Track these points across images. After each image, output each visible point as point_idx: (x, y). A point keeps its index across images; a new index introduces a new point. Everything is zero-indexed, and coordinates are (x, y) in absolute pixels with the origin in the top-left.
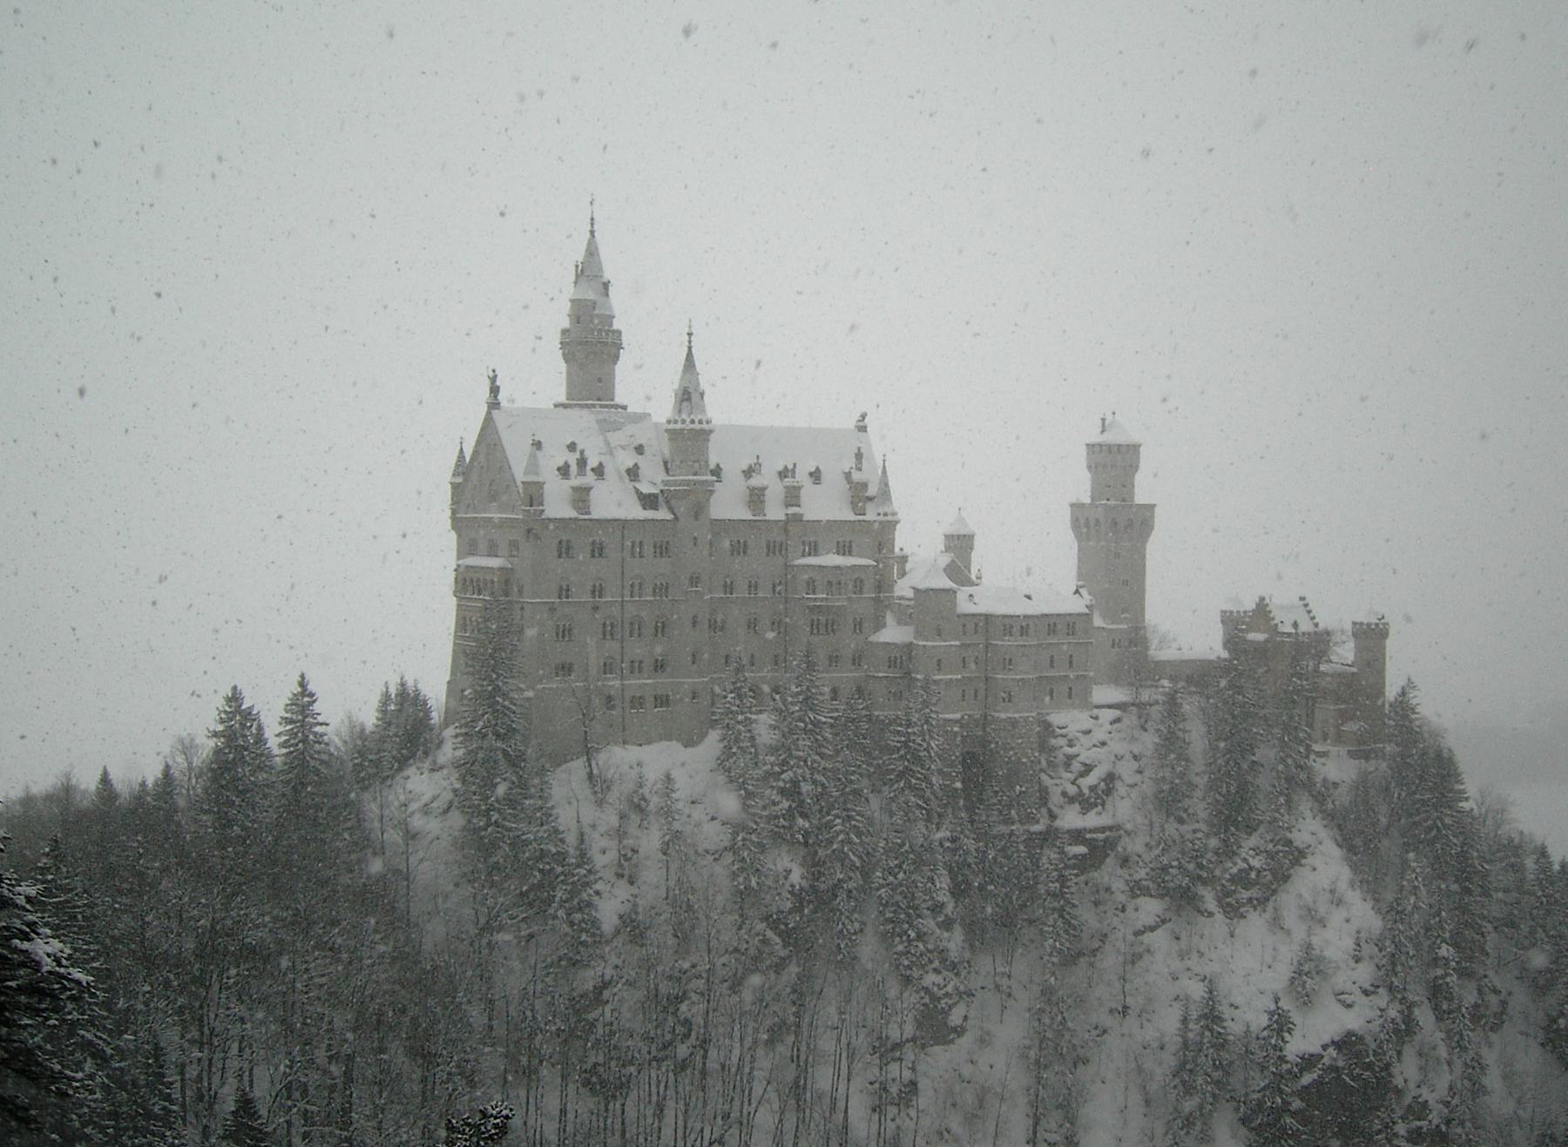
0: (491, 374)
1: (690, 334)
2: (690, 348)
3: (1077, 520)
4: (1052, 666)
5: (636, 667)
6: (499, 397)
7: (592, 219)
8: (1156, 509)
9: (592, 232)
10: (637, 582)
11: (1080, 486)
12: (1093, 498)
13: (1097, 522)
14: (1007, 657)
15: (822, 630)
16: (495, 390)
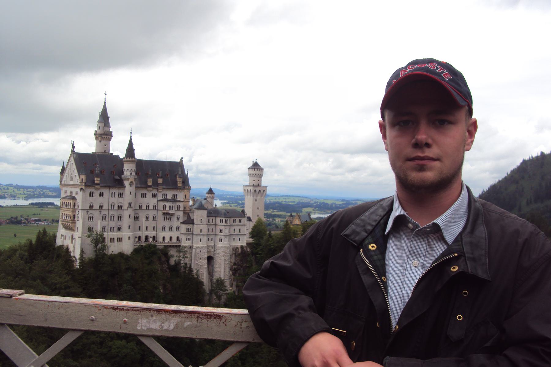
0: (72, 143)
1: (131, 133)
2: (131, 137)
3: (245, 190)
4: (234, 232)
5: (112, 229)
6: (75, 150)
7: (105, 99)
8: (268, 187)
9: (105, 103)
10: (113, 204)
11: (246, 180)
12: (249, 184)
13: (251, 190)
14: (221, 229)
15: (167, 220)
16: (73, 147)
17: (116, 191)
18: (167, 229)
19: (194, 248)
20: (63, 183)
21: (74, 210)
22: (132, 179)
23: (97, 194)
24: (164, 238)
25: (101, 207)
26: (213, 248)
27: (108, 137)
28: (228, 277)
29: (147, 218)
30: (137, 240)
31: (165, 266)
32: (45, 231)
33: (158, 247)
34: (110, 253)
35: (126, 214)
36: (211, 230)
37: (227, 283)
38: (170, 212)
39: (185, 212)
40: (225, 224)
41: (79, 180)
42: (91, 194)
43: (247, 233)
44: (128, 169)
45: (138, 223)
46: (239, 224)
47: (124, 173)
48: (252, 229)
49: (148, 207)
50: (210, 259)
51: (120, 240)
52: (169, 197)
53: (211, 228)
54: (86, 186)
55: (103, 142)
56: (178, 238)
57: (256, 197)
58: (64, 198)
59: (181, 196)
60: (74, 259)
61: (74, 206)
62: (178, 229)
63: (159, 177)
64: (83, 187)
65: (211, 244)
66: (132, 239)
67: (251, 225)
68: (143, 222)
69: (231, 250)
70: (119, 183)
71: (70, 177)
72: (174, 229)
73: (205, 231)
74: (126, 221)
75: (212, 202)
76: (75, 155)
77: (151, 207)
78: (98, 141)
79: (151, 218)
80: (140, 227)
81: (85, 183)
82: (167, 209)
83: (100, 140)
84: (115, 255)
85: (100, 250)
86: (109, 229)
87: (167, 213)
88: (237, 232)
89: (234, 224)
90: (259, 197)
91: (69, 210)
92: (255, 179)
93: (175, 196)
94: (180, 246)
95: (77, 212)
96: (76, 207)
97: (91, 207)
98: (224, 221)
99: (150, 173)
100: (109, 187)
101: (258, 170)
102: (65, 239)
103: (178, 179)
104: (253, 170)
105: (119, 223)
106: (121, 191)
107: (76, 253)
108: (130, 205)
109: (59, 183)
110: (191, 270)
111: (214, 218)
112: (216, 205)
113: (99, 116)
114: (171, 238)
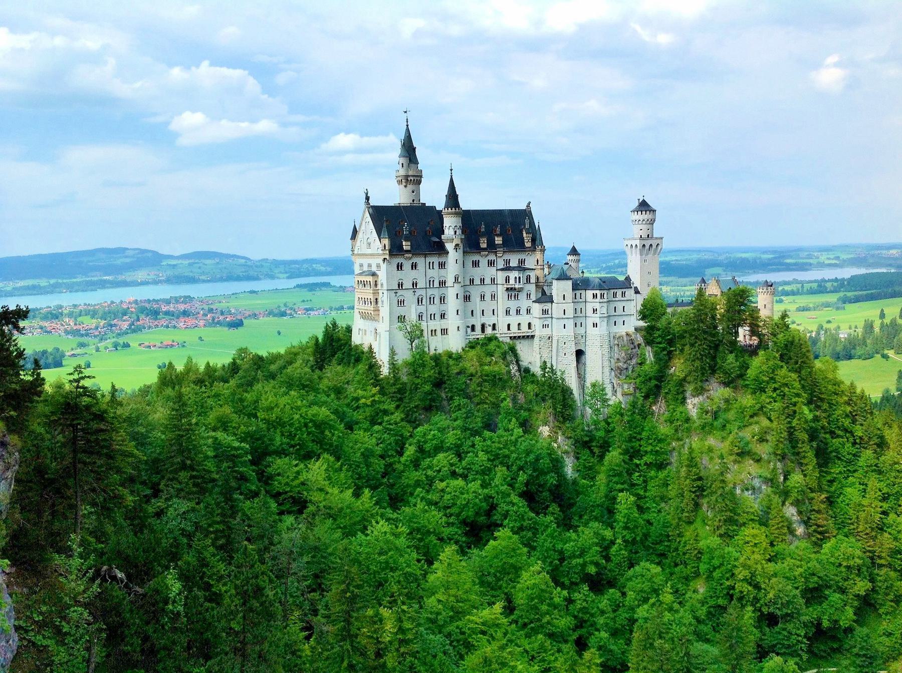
5: (432, 317)
9: (407, 125)
16: (367, 198)
17: (435, 260)
18: (513, 312)
19: (555, 339)
20: (356, 252)
21: (376, 293)
22: (457, 241)
23: (407, 265)
24: (509, 325)
25: (415, 285)
26: (584, 337)
27: (416, 179)
28: (607, 381)
29: (483, 297)
30: (469, 330)
31: (514, 368)
32: (335, 325)
33: (501, 339)
34: (432, 352)
35: (452, 292)
36: (579, 310)
37: (609, 390)
38: (517, 286)
39: (537, 285)
40: (601, 301)
41: (381, 246)
42: (400, 267)
43: (633, 311)
44: (451, 225)
45: (470, 306)
46: (623, 299)
47: (446, 231)
48: (642, 305)
50: (579, 354)
51: (444, 332)
52: (514, 263)
53: (578, 307)
54: (391, 254)
55: (410, 187)
56: (529, 324)
57: (647, 254)
58: (361, 274)
59: (530, 262)
60: (381, 363)
61: (376, 285)
62: (528, 311)
63: (498, 235)
64: (387, 257)
65: (581, 331)
66: (462, 329)
67: (639, 300)
68: (477, 304)
69: (612, 338)
70: (439, 249)
71: (365, 243)
72: (523, 311)
73: (570, 313)
74: (453, 304)
75: (578, 267)
76: (371, 210)
77: (488, 281)
78: (402, 186)
80: (472, 311)
81: (390, 251)
82: (512, 281)
83: (404, 184)
84: (440, 354)
85: (417, 348)
86: (429, 316)
87: (512, 288)
88: (620, 311)
89: (614, 299)
90: (650, 256)
91: (368, 291)
92: (641, 227)
93: (522, 262)
94: (533, 337)
95: (381, 294)
96: (379, 287)
97: (400, 285)
98: (599, 296)
99: (483, 230)
100: (425, 256)
101: (648, 212)
102: (365, 334)
103: (525, 235)
104: (640, 213)
105: (443, 307)
106: (442, 260)
107: (383, 357)
108: (456, 279)
109: (351, 253)
110: (552, 370)
111: (583, 292)
112: (583, 272)
113: (400, 147)
114: (519, 324)
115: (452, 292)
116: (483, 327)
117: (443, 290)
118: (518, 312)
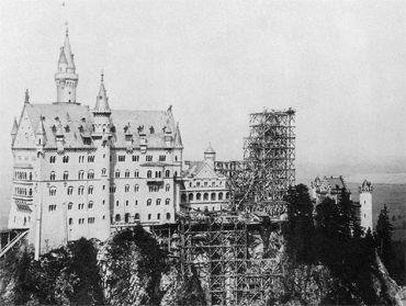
5: (81, 206)
16: (27, 98)
18: (154, 202)
23: (59, 159)
24: (150, 216)
25: (66, 176)
29: (127, 189)
38: (158, 180)
42: (53, 160)
49: (127, 174)
61: (31, 177)
68: (120, 195)
74: (101, 194)
79: (132, 189)
82: (153, 175)
97: (53, 177)
115: (100, 183)
116: (127, 215)
117: (90, 183)
118: (158, 202)
